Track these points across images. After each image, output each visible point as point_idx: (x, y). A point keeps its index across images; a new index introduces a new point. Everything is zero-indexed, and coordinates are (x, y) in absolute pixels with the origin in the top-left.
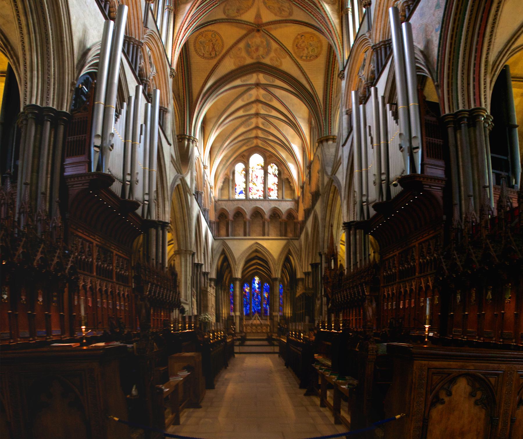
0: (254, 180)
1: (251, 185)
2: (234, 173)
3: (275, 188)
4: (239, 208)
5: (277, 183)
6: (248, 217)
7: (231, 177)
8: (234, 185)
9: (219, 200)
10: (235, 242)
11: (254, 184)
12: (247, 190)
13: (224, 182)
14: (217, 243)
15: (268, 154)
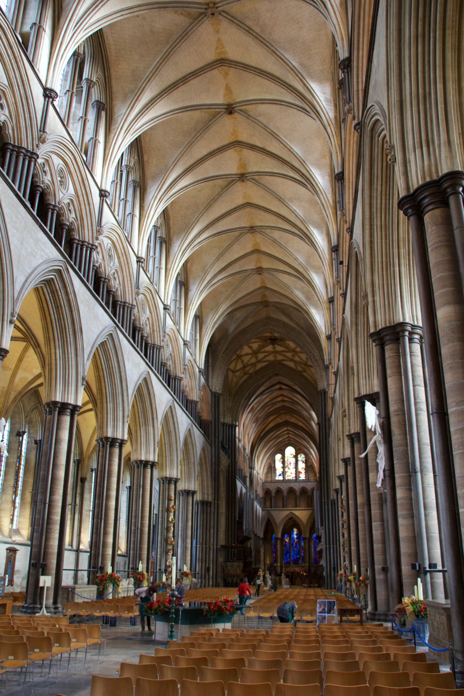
0: (289, 466)
1: (286, 469)
2: (274, 462)
3: (303, 471)
4: (279, 488)
5: (304, 467)
6: (285, 494)
7: (273, 465)
8: (275, 470)
9: (265, 482)
10: (277, 512)
11: (289, 469)
12: (284, 473)
13: (268, 469)
14: (264, 512)
15: (298, 448)
